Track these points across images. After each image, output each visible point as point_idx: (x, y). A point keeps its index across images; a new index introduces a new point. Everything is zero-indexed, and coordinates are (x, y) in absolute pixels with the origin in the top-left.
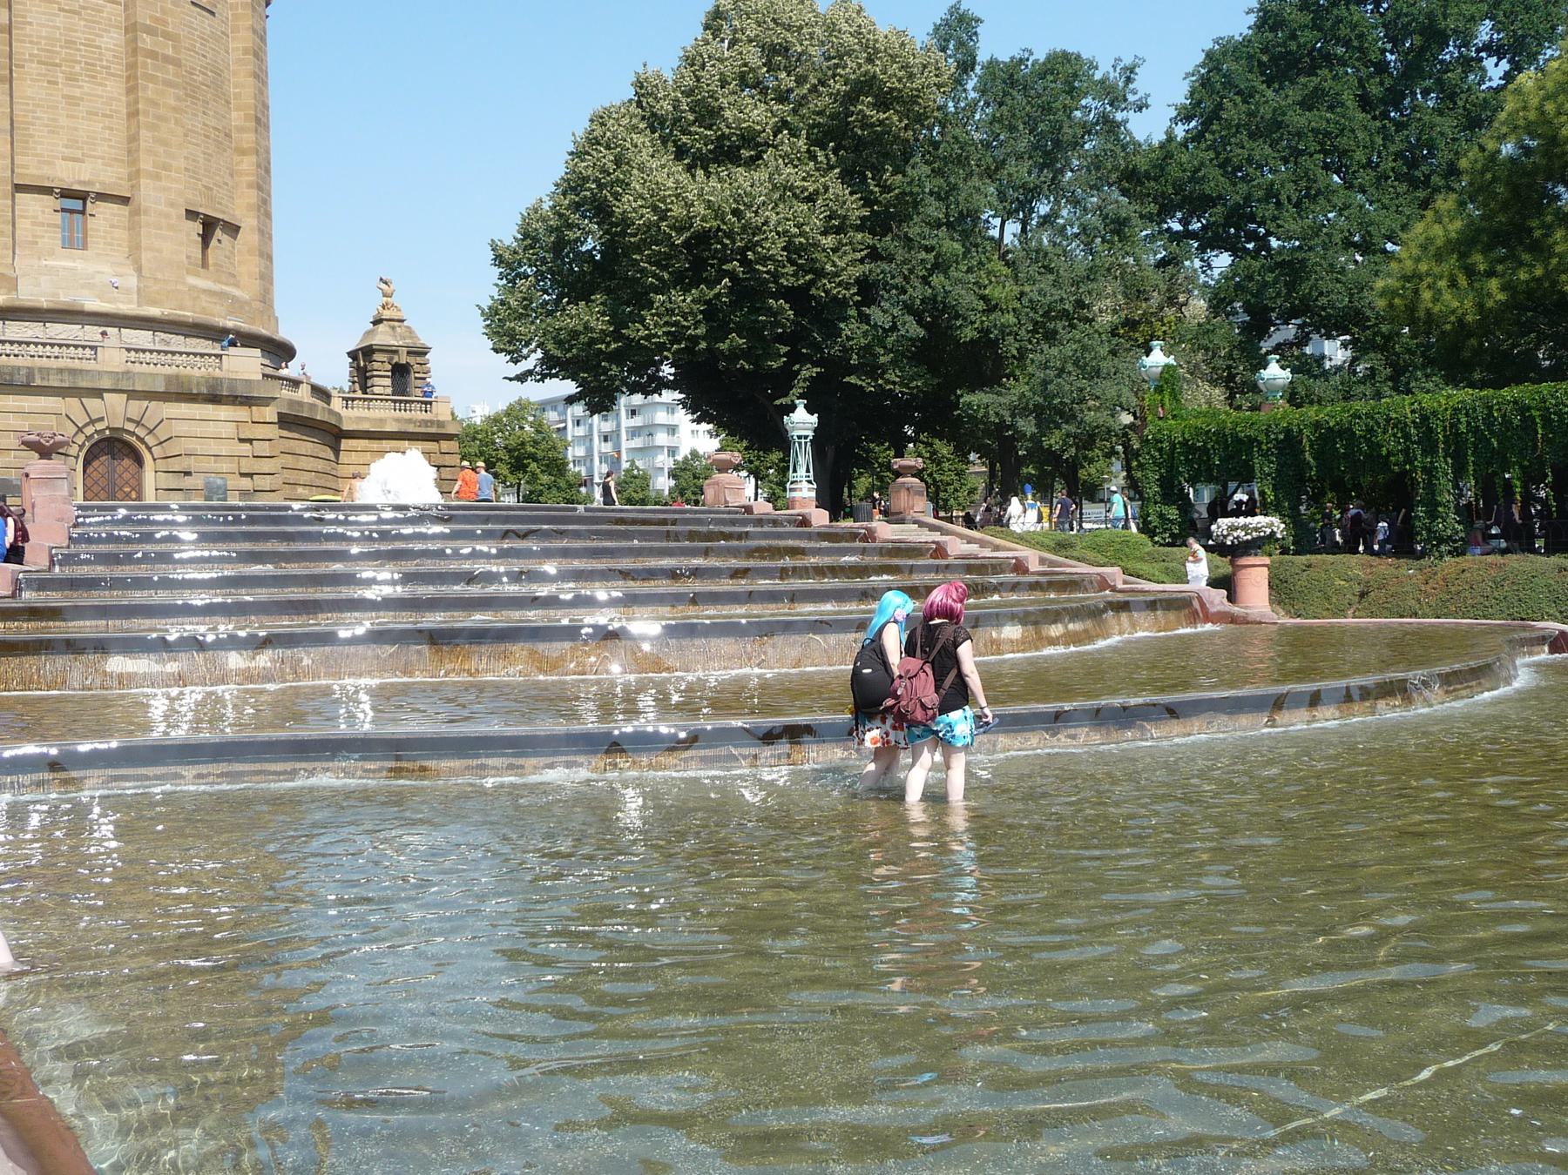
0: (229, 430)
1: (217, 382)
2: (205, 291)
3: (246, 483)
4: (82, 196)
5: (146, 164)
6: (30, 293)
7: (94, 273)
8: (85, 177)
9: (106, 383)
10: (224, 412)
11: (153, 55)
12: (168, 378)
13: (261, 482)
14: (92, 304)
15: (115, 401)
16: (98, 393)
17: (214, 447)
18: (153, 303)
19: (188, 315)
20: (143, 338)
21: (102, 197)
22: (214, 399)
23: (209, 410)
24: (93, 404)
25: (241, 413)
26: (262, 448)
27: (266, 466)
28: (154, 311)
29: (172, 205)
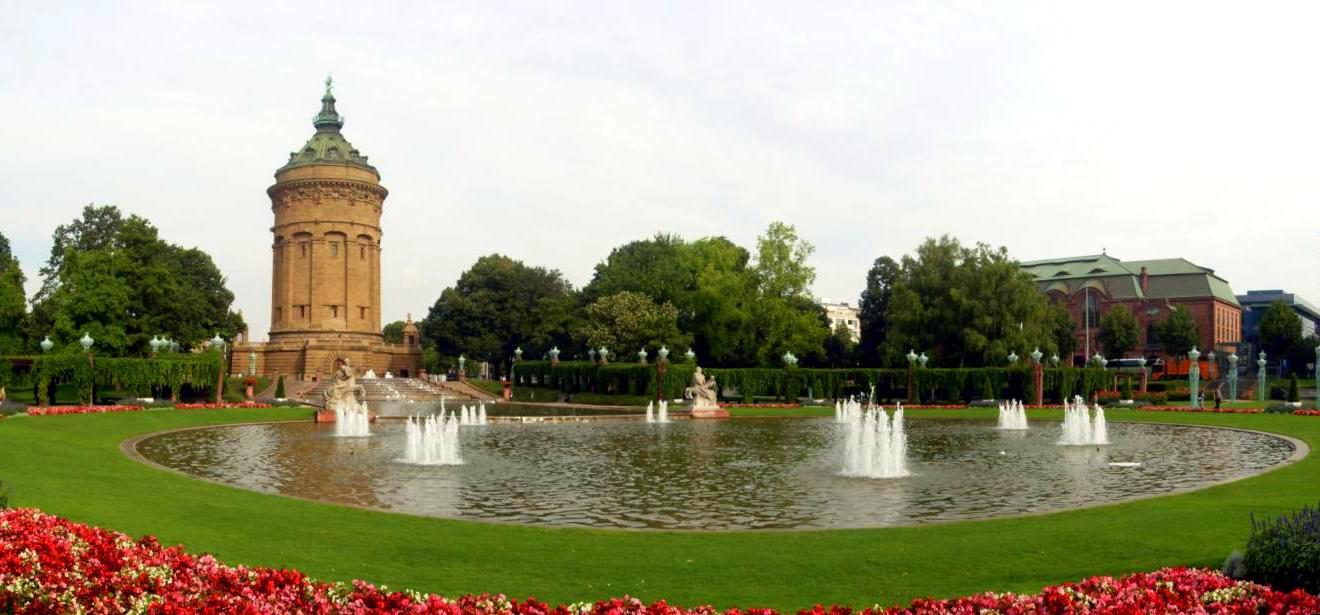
6: (326, 327)
7: (338, 323)
10: (361, 354)
15: (340, 352)
19: (356, 330)
23: (356, 353)
25: (365, 353)
28: (349, 330)
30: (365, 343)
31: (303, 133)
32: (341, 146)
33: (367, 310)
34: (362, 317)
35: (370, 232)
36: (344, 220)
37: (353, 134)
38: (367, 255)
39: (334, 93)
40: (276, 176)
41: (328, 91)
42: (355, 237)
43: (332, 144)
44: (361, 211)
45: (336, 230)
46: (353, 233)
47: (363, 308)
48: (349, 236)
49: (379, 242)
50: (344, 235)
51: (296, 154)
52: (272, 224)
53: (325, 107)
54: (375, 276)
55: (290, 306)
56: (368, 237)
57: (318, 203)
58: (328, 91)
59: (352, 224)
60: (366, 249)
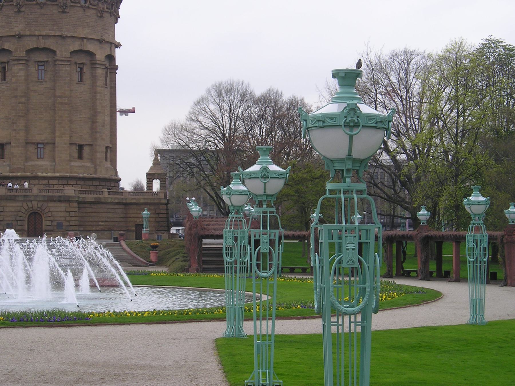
0: (63, 209)
1: (60, 196)
2: (76, 166)
3: (67, 223)
5: (58, 134)
8: (43, 138)
9: (32, 198)
10: (63, 205)
11: (61, 103)
12: (47, 196)
13: (71, 223)
14: (40, 174)
15: (35, 203)
16: (31, 201)
17: (60, 214)
18: (58, 172)
20: (55, 182)
21: (46, 143)
22: (60, 201)
24: (30, 204)
25: (67, 205)
26: (72, 214)
27: (73, 219)
28: (58, 175)
29: (66, 144)
30: (69, 191)
33: (86, 150)
34: (80, 157)
35: (90, 47)
36: (53, 33)
42: (68, 55)
45: (42, 46)
47: (81, 147)
48: (58, 52)
49: (111, 58)
50: (54, 52)
57: (19, 12)
59: (62, 37)
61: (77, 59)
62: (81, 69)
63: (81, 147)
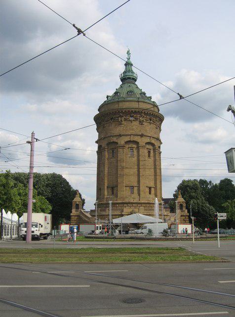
4: (133, 187)
31: (112, 85)
32: (136, 91)
33: (153, 190)
35: (153, 141)
37: (143, 84)
38: (152, 154)
39: (132, 61)
40: (99, 110)
41: (129, 59)
43: (130, 89)
44: (148, 128)
46: (142, 141)
49: (159, 147)
51: (110, 96)
52: (97, 138)
53: (126, 68)
54: (158, 171)
55: (106, 187)
56: (153, 145)
58: (129, 59)
60: (152, 151)
61: (148, 146)
62: (149, 152)
63: (150, 188)
